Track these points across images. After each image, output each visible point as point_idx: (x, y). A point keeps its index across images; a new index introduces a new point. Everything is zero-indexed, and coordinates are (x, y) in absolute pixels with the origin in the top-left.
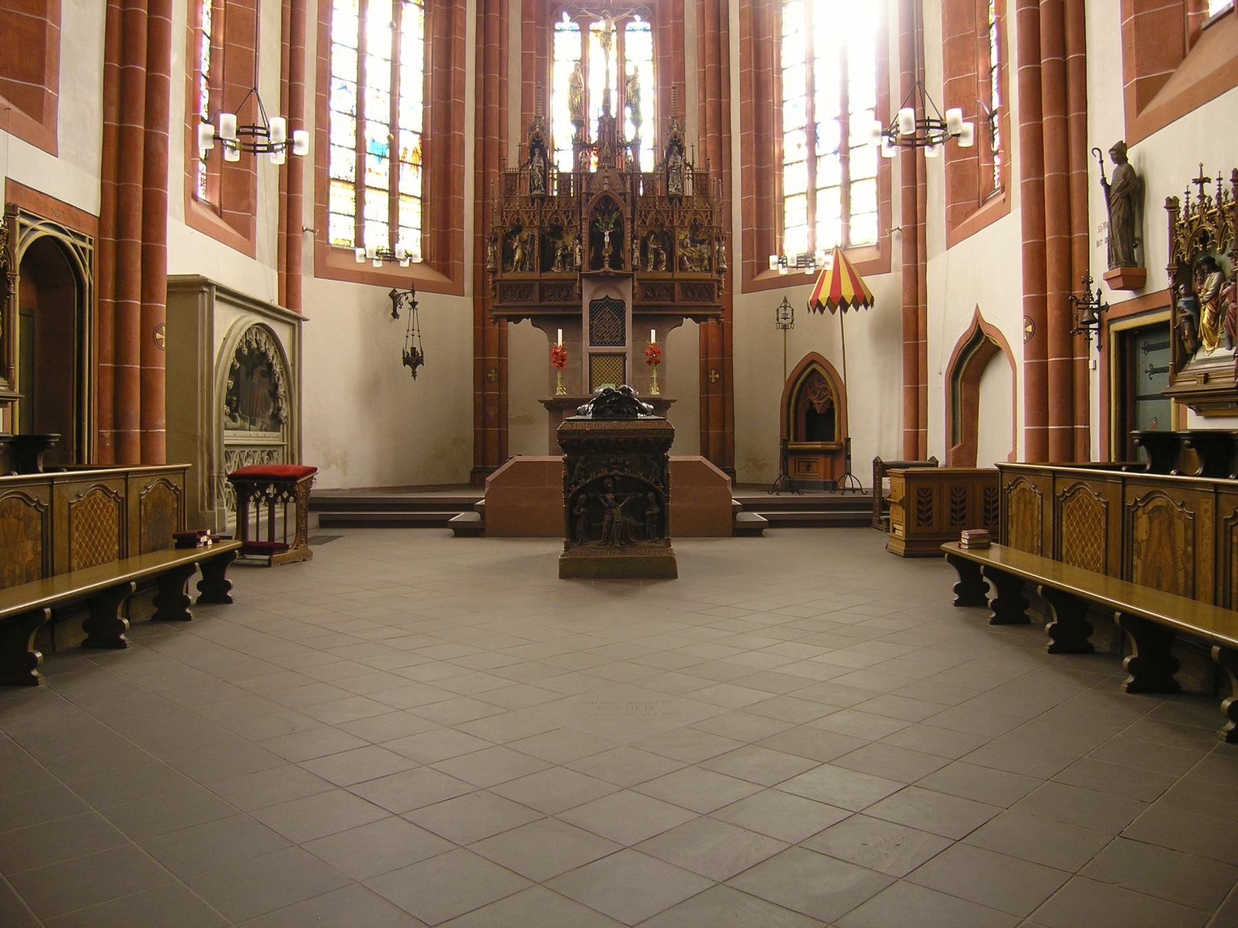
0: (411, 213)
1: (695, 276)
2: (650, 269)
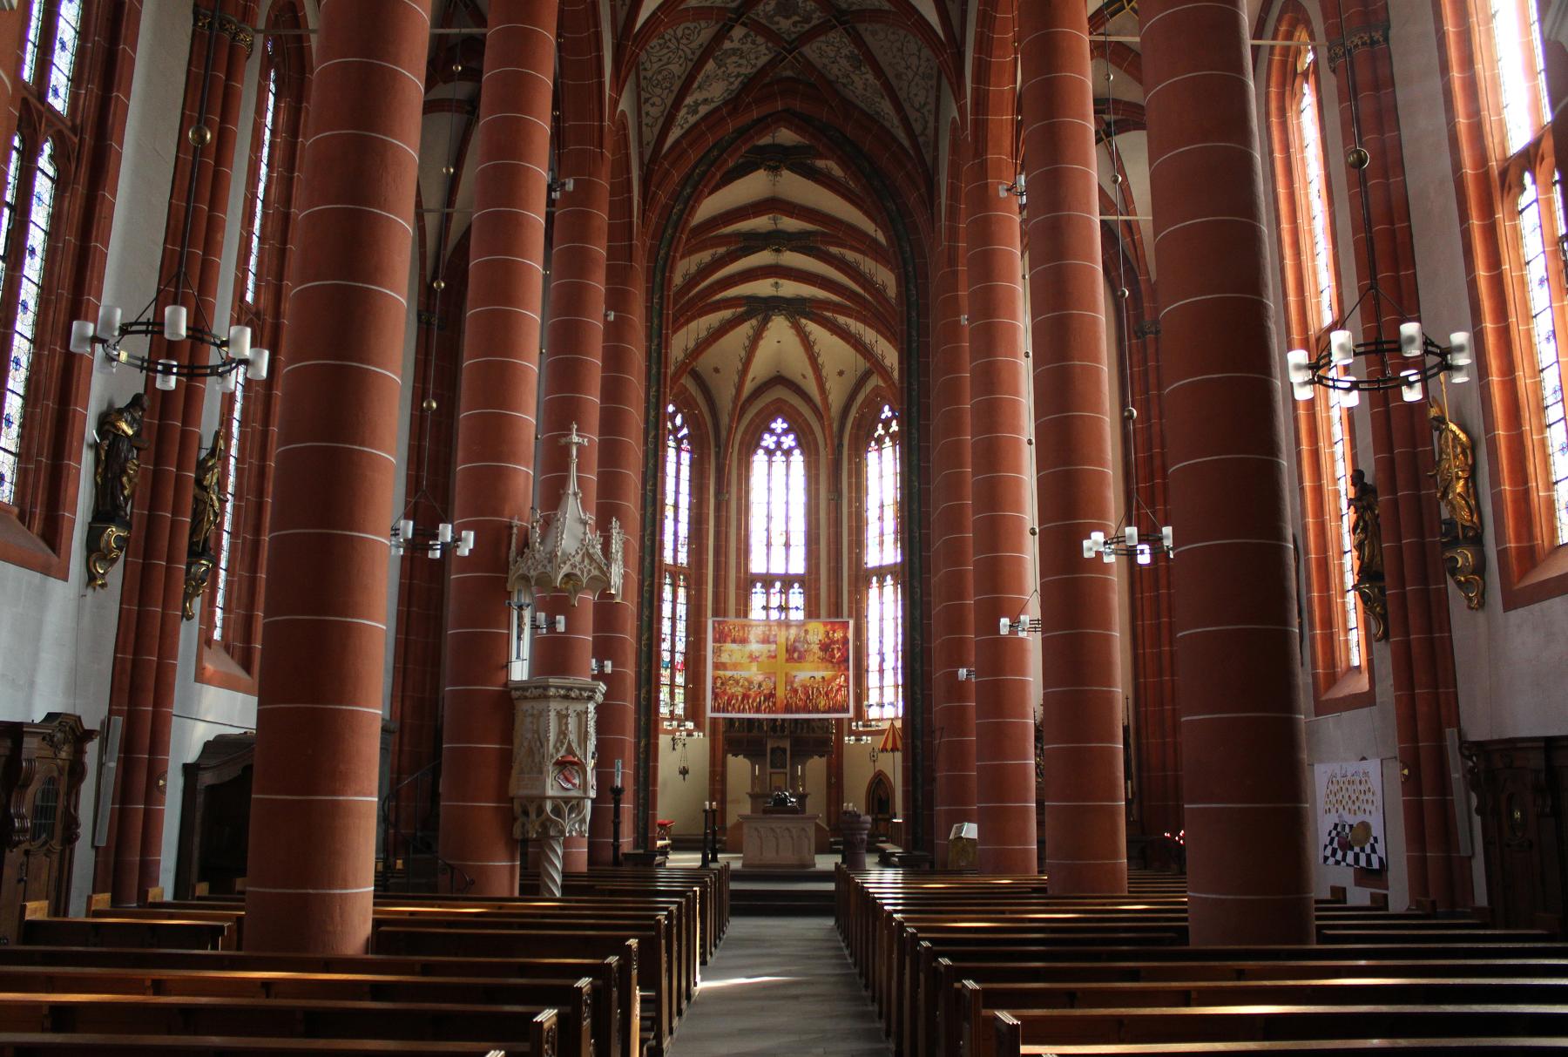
0: (680, 695)
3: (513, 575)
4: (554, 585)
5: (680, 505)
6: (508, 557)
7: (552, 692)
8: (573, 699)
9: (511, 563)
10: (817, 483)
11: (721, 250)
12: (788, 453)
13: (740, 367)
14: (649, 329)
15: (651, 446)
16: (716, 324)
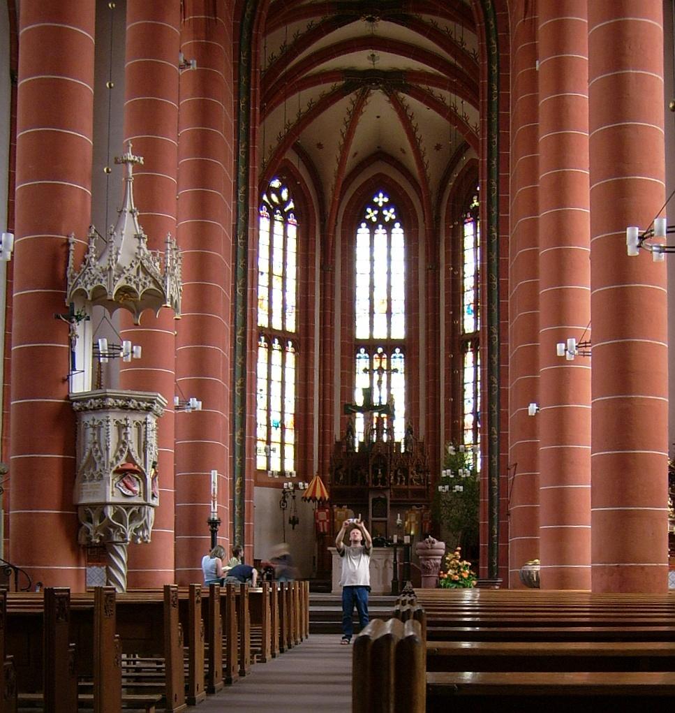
0: (290, 452)
1: (417, 487)
2: (398, 484)
3: (70, 292)
4: (109, 298)
5: (288, 275)
6: (66, 274)
7: (110, 402)
8: (131, 409)
9: (69, 279)
10: (417, 254)
11: (317, 20)
12: (389, 226)
13: (342, 143)
14: (238, 85)
15: (241, 201)
16: (316, 99)
